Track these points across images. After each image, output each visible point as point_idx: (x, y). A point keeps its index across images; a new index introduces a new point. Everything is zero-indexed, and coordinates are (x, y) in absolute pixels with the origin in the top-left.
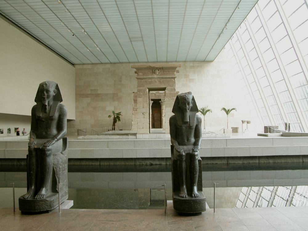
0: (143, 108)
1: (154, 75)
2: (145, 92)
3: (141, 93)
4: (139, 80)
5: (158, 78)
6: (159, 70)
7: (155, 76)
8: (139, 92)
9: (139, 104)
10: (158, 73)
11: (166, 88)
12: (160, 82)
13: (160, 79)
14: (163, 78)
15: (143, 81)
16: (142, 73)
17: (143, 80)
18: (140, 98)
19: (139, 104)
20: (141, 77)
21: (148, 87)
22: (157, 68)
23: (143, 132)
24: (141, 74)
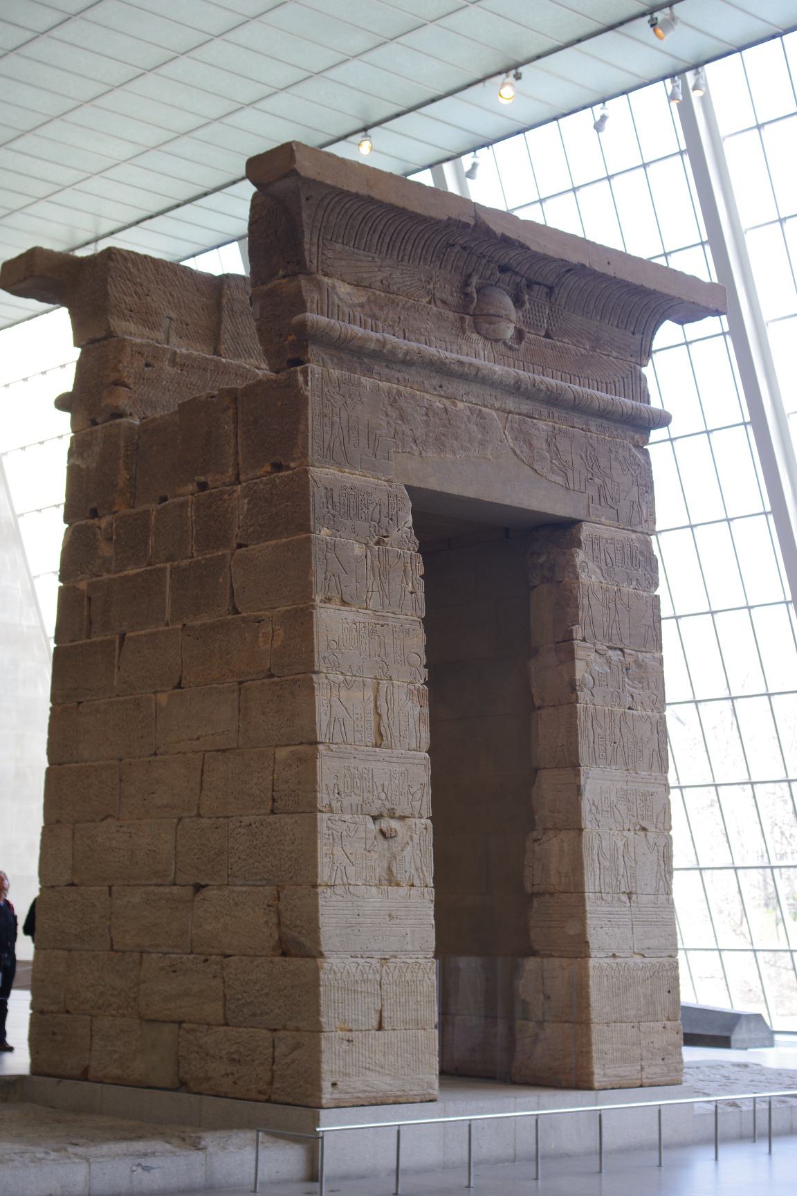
0: (380, 739)
1: (475, 336)
2: (395, 534)
3: (358, 550)
4: (336, 373)
5: (516, 389)
6: (518, 303)
7: (477, 355)
8: (335, 529)
9: (332, 685)
10: (509, 333)
11: (586, 531)
12: (523, 436)
13: (526, 407)
14: (553, 400)
15: (366, 381)
16: (357, 285)
17: (369, 372)
18: (349, 614)
19: (332, 685)
20: (357, 330)
21: (416, 484)
22: (504, 269)
23: (383, 1083)
24: (343, 289)
